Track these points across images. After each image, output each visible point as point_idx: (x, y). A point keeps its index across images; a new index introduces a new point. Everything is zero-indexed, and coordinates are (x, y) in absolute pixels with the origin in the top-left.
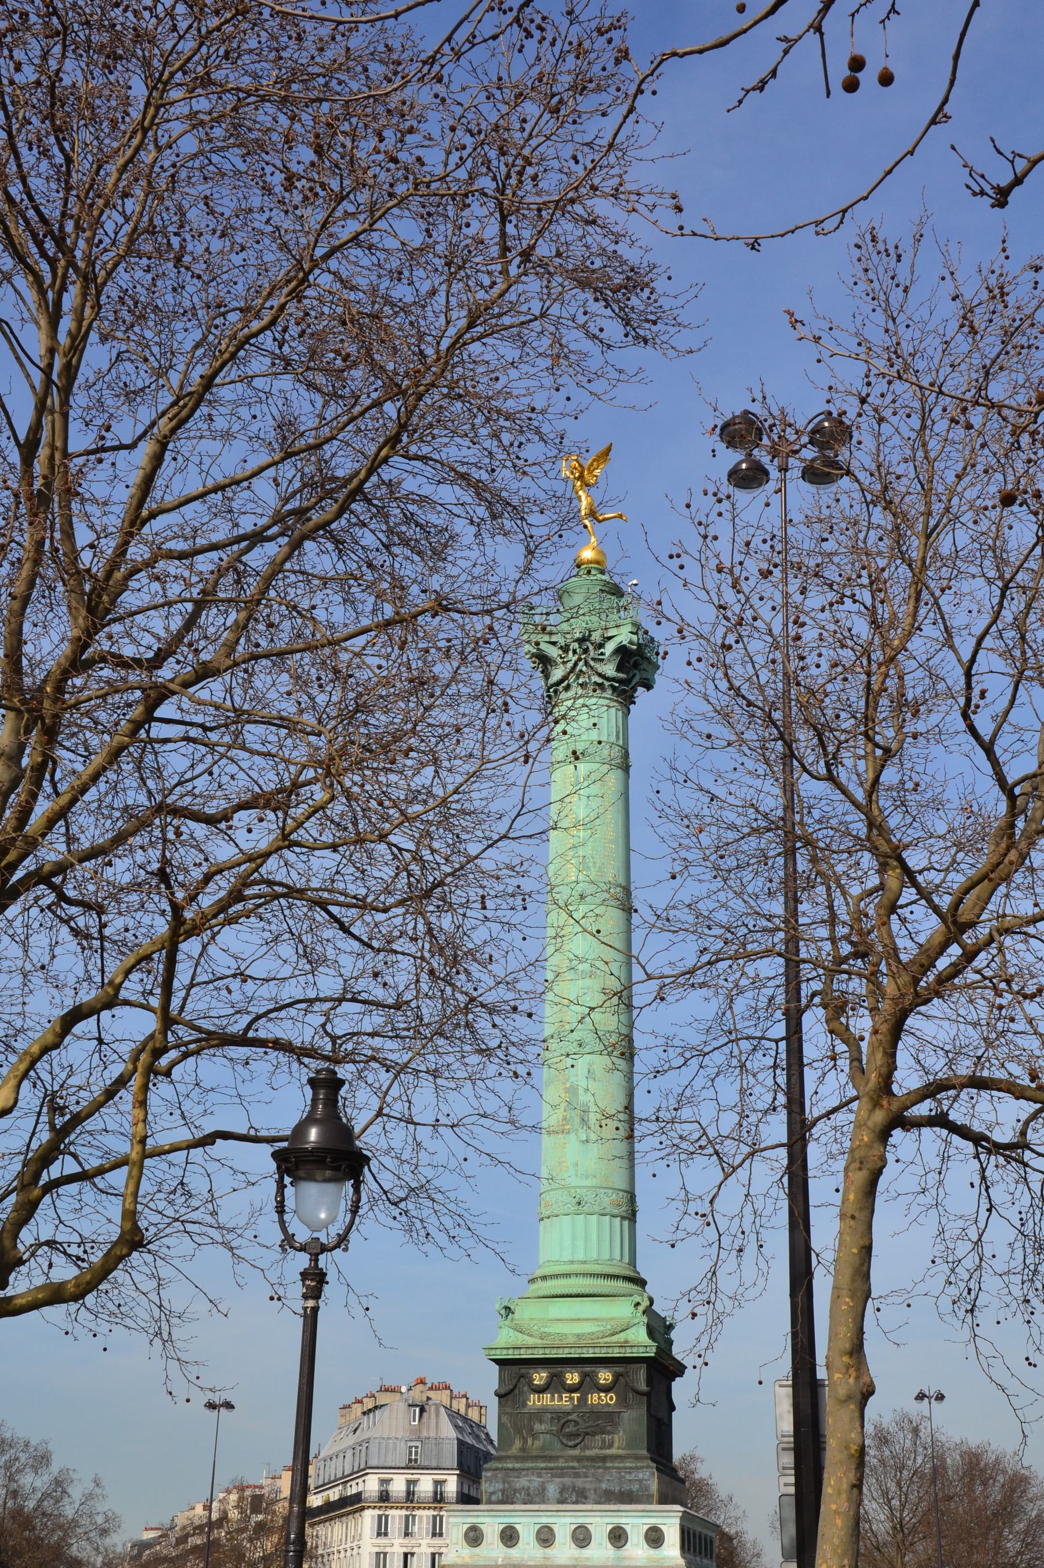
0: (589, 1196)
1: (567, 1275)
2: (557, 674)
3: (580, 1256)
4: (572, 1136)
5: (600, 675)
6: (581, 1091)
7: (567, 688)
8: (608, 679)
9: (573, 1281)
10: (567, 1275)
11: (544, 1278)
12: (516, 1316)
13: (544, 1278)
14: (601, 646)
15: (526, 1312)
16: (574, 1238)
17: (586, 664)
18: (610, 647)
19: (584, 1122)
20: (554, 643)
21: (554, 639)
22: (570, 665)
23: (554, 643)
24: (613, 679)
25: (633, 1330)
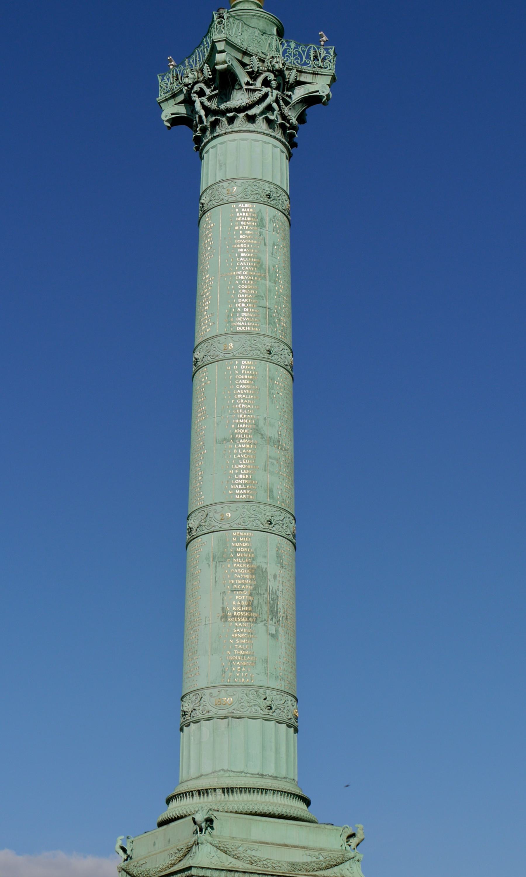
0: (277, 699)
1: (263, 791)
2: (239, 99)
3: (271, 771)
4: (260, 626)
5: (284, 117)
6: (270, 577)
7: (252, 119)
9: (269, 798)
10: (263, 791)
11: (228, 790)
12: (214, 832)
13: (228, 790)
14: (291, 88)
15: (226, 828)
16: (263, 748)
17: (277, 101)
18: (299, 93)
19: (273, 613)
20: (244, 65)
21: (246, 60)
22: (257, 95)
23: (244, 65)
25: (347, 865)
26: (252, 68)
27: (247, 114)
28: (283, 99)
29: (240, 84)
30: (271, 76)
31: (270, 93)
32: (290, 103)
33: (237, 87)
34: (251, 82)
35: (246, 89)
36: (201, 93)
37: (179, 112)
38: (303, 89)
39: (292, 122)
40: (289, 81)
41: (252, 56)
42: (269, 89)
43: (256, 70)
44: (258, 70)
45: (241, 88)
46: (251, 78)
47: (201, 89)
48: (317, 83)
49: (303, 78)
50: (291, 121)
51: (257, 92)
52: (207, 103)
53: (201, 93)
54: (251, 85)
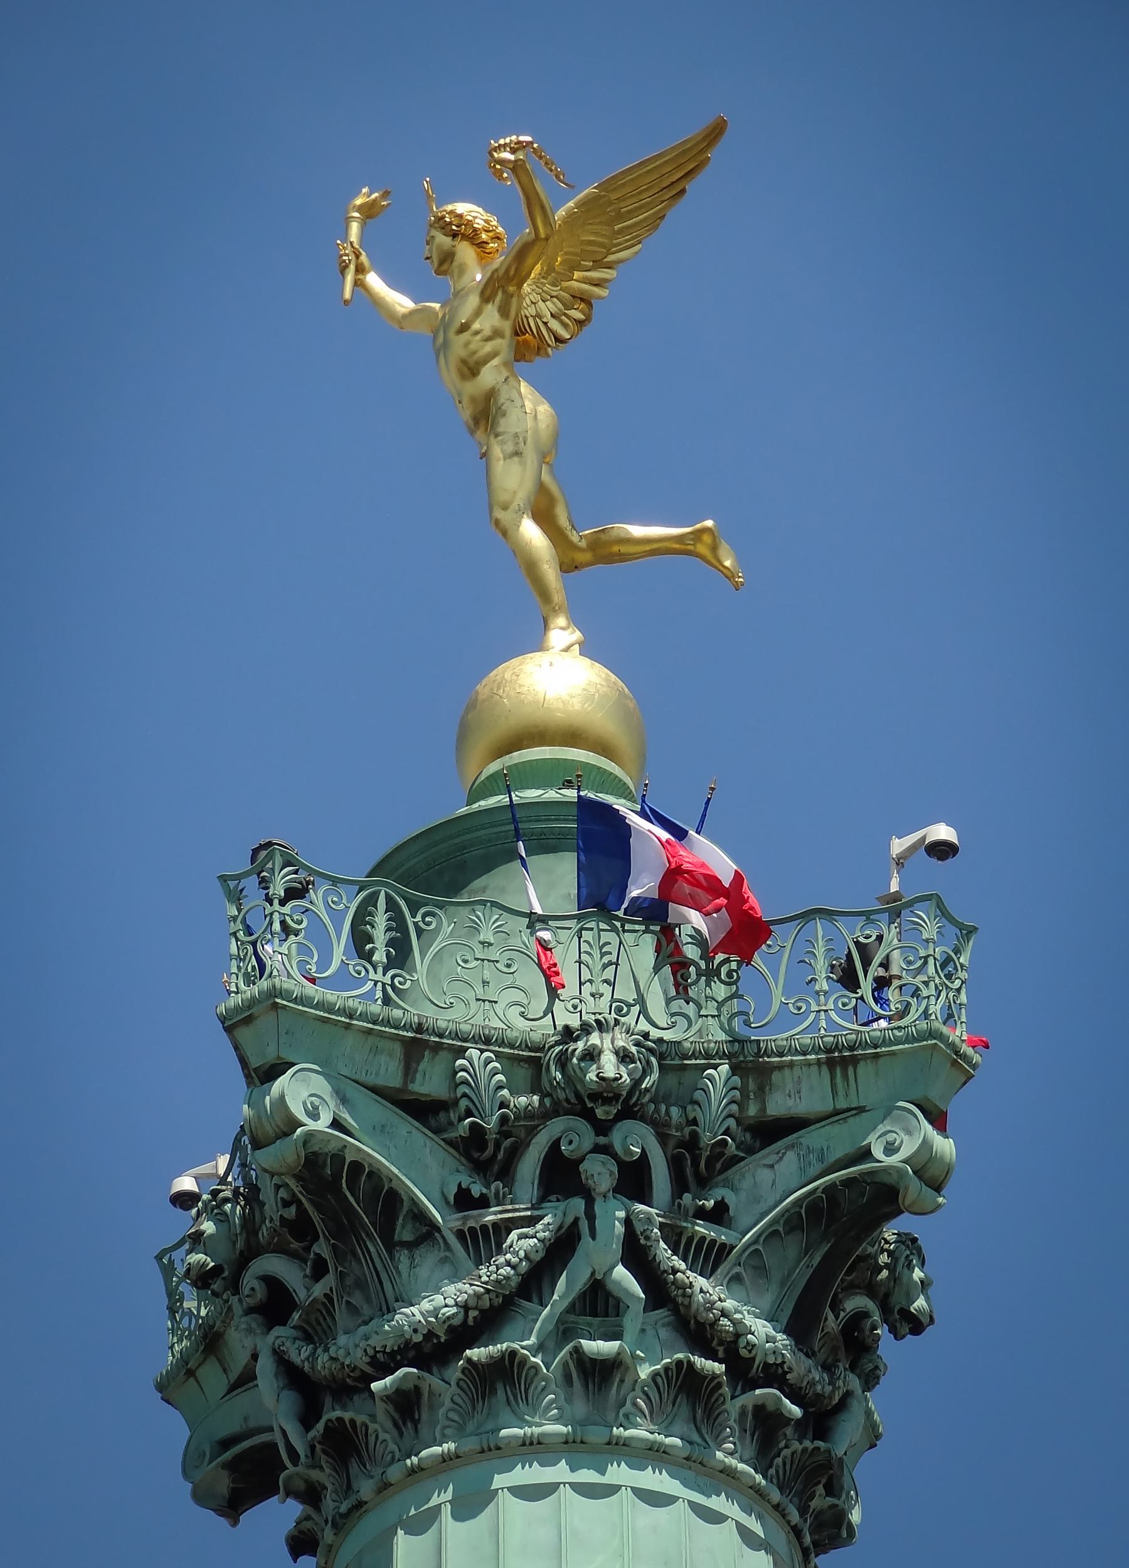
5: (698, 1332)
8: (745, 1370)
20: (424, 1111)
21: (429, 1083)
24: (774, 1375)
26: (469, 1113)
27: (469, 1360)
28: (675, 1238)
29: (420, 1216)
30: (575, 1136)
31: (584, 1226)
32: (724, 1250)
33: (404, 1232)
34: (477, 1190)
35: (460, 1234)
36: (275, 1305)
37: (252, 1424)
38: (791, 1155)
39: (751, 1346)
40: (694, 1136)
41: (461, 1052)
42: (577, 1205)
43: (491, 1124)
44: (504, 1119)
45: (428, 1232)
46: (481, 1168)
47: (272, 1283)
48: (861, 1110)
49: (779, 1105)
50: (742, 1343)
51: (514, 1235)
52: (299, 1354)
53: (275, 1305)
54: (483, 1203)
